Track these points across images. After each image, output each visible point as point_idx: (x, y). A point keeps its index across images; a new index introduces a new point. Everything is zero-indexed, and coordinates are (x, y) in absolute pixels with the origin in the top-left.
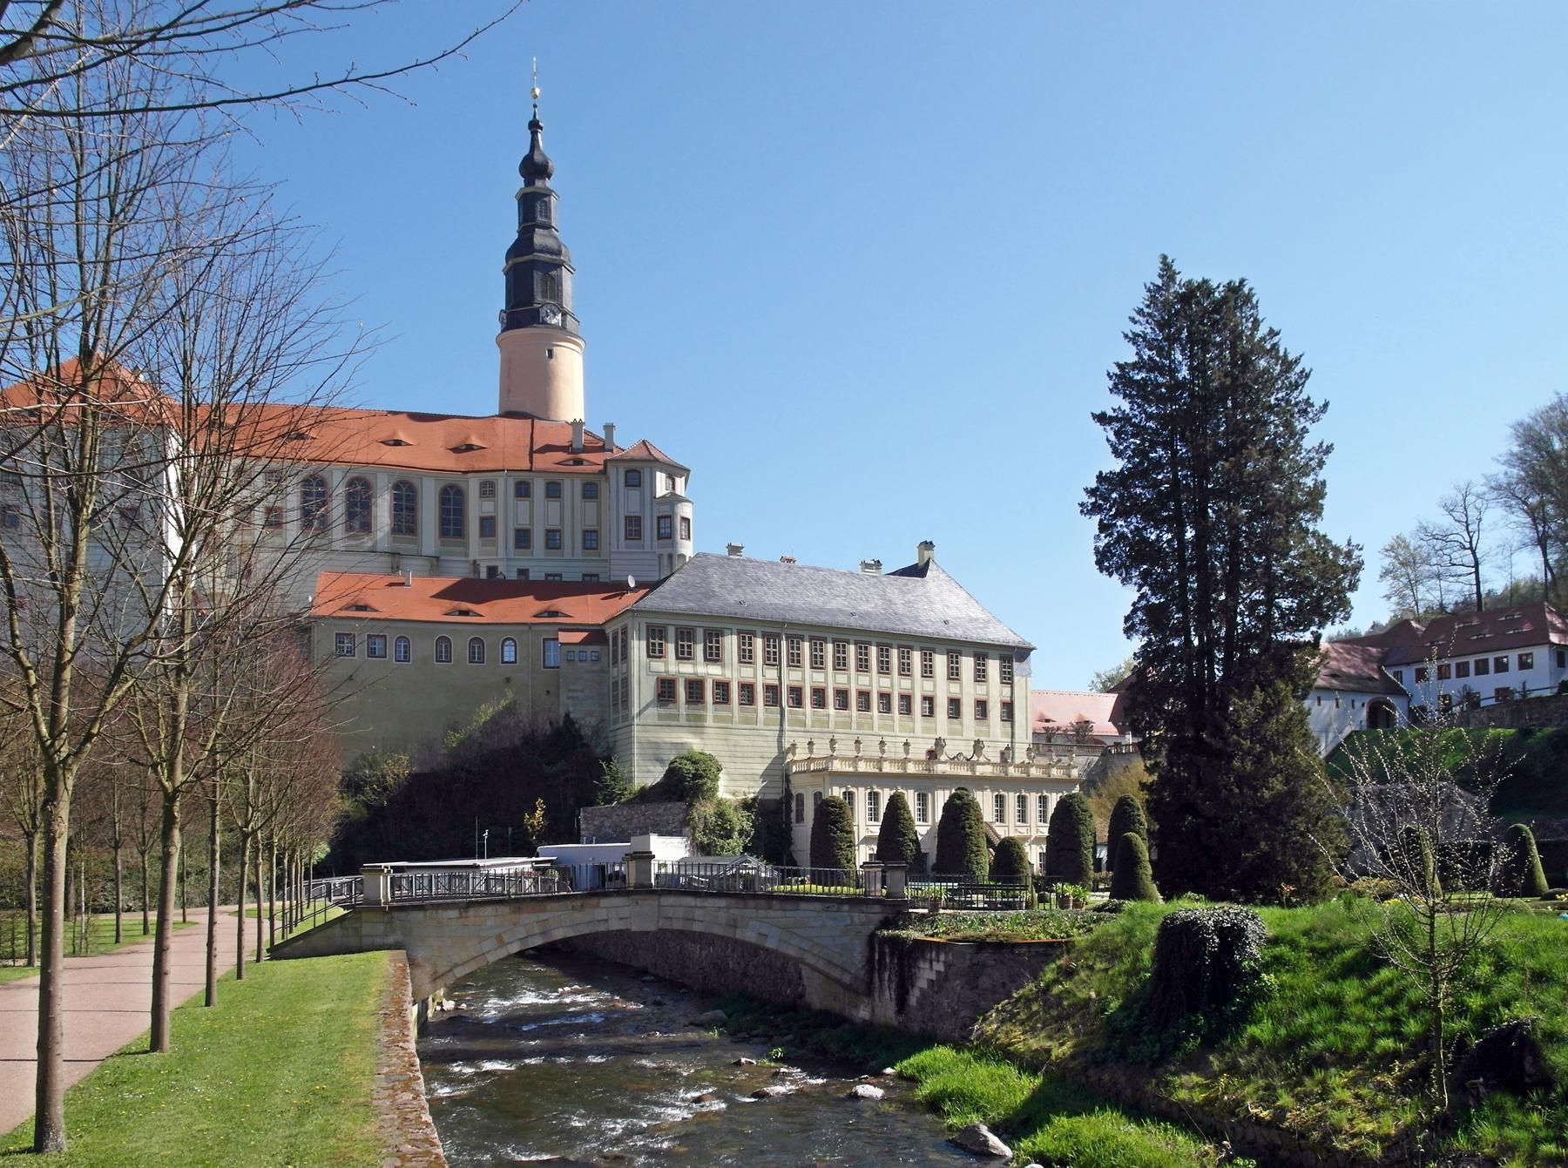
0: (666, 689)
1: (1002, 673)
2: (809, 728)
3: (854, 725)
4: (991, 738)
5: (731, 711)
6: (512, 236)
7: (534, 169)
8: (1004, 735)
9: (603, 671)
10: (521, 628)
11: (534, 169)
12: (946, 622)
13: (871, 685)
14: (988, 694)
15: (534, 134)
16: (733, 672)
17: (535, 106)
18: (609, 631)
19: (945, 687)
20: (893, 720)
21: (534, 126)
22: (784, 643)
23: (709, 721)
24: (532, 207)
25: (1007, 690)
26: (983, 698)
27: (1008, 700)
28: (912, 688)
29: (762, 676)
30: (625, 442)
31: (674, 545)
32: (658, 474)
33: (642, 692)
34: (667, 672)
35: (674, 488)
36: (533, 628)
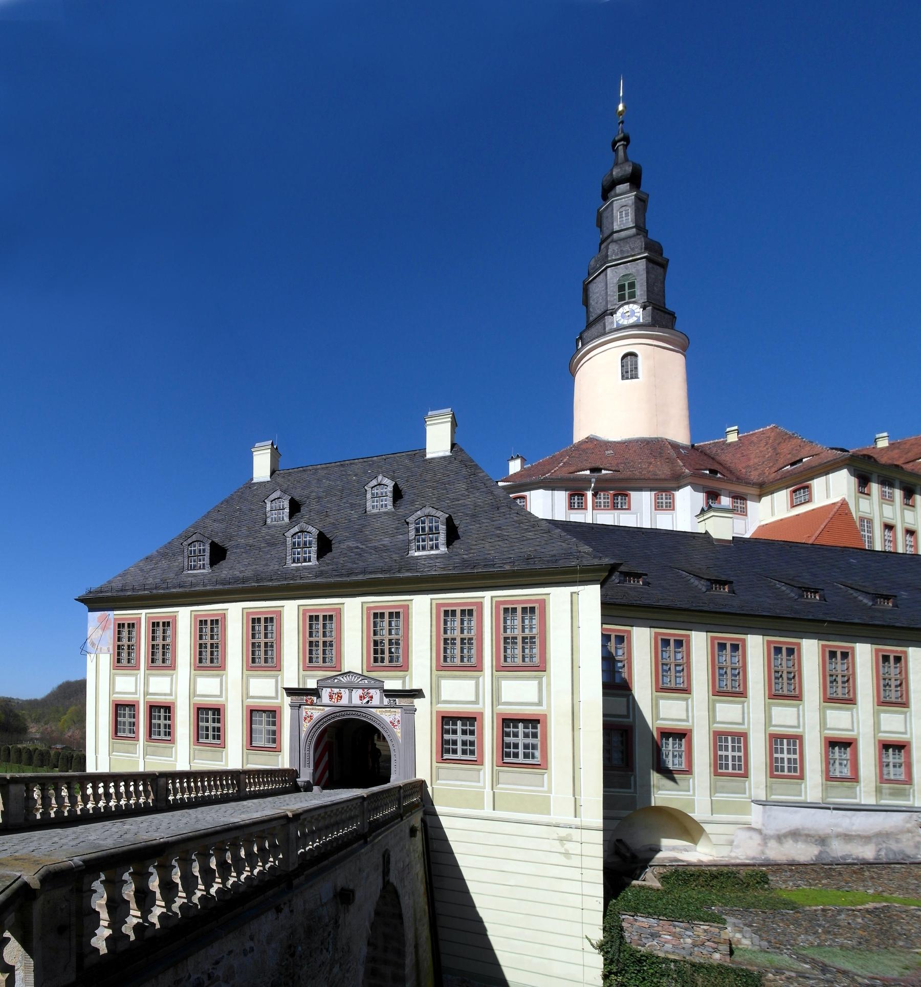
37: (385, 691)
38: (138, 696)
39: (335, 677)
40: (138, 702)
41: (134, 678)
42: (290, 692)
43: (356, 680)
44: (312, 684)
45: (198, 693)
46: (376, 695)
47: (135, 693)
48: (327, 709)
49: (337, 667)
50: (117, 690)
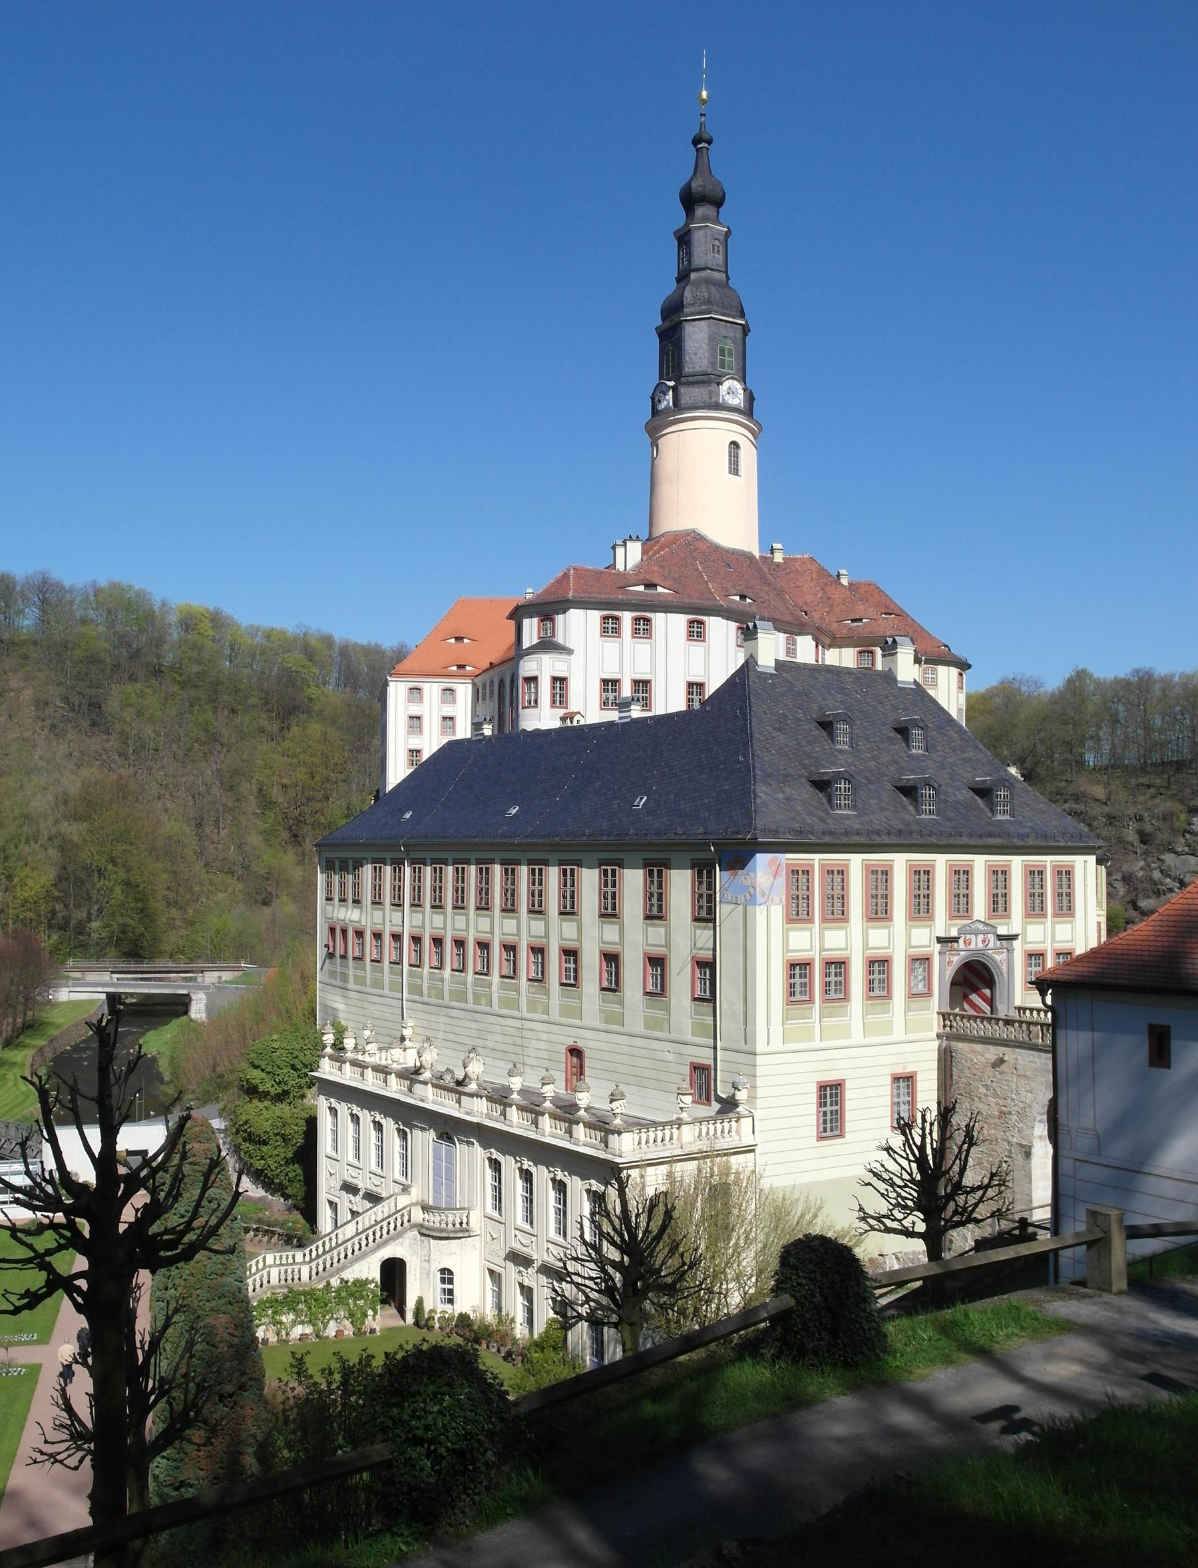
1: (697, 897)
2: (426, 999)
3: (470, 997)
4: (674, 1036)
5: (364, 969)
8: (698, 1029)
13: (492, 932)
14: (668, 945)
19: (595, 932)
20: (517, 990)
22: (408, 870)
23: (351, 985)
25: (705, 935)
26: (659, 951)
27: (707, 955)
28: (547, 936)
32: (526, 622)
34: (332, 919)
35: (553, 635)
37: (998, 936)
38: (813, 953)
39: (968, 925)
40: (813, 959)
41: (809, 933)
42: (940, 940)
43: (981, 926)
44: (954, 933)
45: (870, 946)
46: (991, 937)
47: (811, 950)
48: (962, 953)
49: (970, 918)
50: (791, 948)
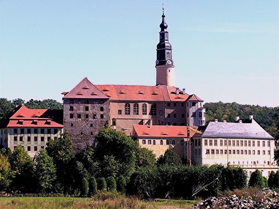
0: (208, 152)
6: (158, 42)
7: (163, 27)
9: (193, 147)
10: (176, 138)
11: (163, 27)
12: (257, 134)
15: (163, 18)
16: (219, 147)
17: (163, 12)
18: (194, 139)
21: (163, 16)
24: (163, 36)
26: (264, 150)
29: (224, 148)
30: (189, 92)
31: (202, 119)
33: (204, 151)
36: (179, 138)
